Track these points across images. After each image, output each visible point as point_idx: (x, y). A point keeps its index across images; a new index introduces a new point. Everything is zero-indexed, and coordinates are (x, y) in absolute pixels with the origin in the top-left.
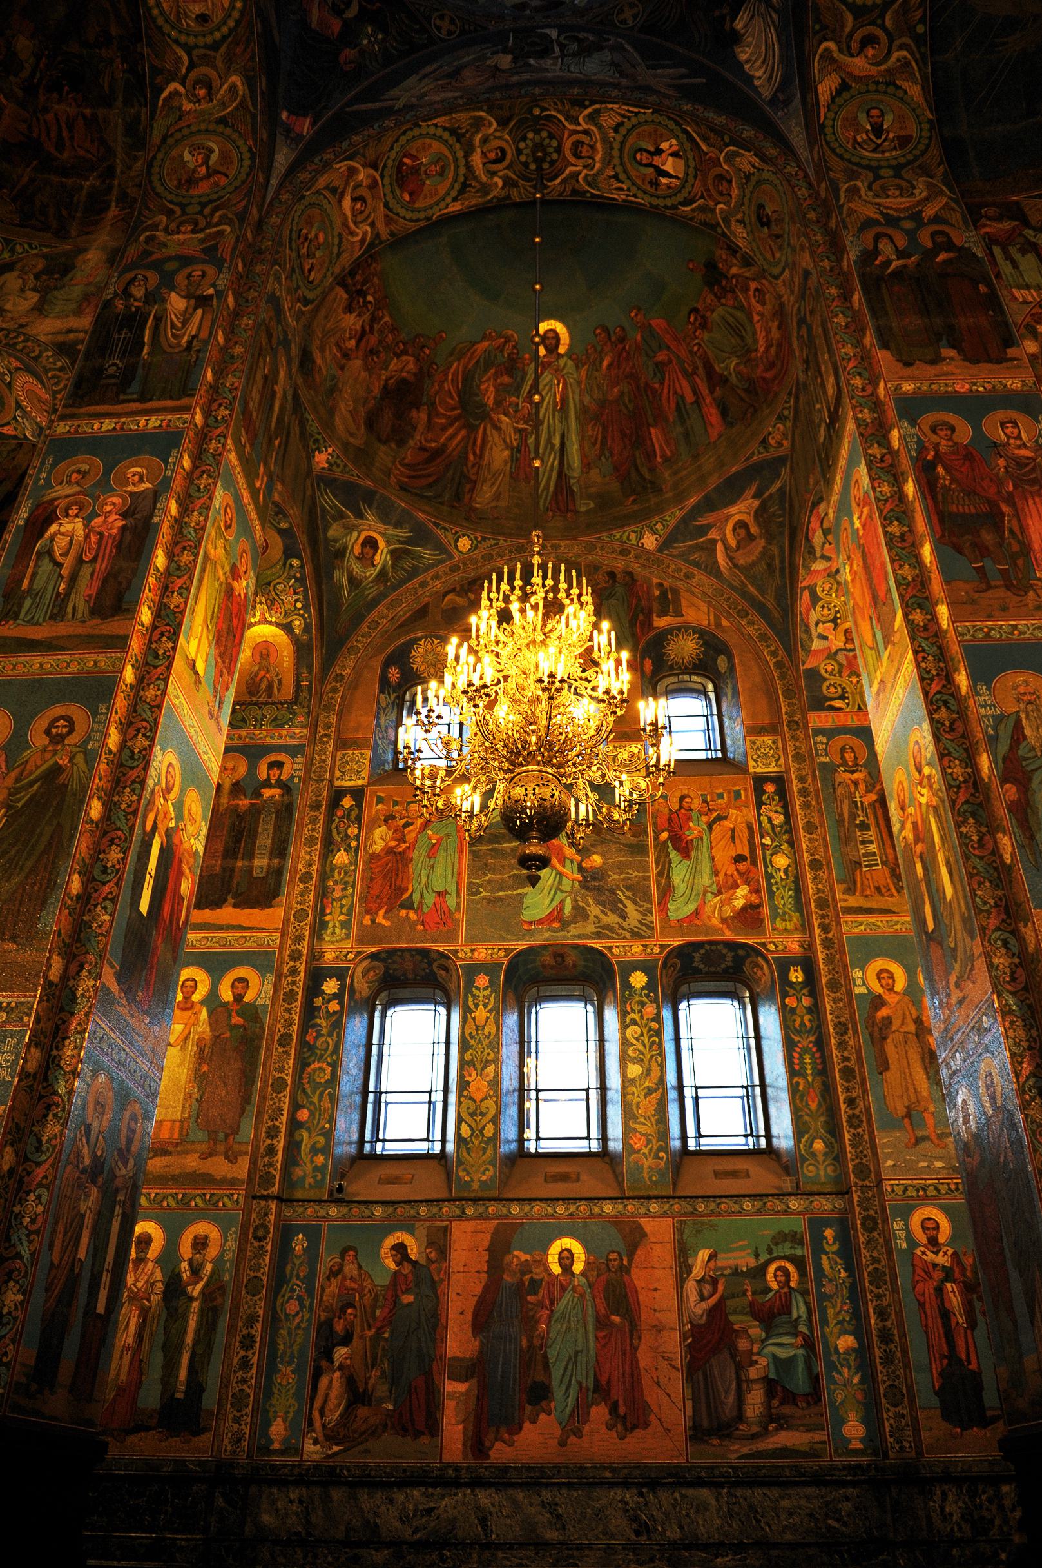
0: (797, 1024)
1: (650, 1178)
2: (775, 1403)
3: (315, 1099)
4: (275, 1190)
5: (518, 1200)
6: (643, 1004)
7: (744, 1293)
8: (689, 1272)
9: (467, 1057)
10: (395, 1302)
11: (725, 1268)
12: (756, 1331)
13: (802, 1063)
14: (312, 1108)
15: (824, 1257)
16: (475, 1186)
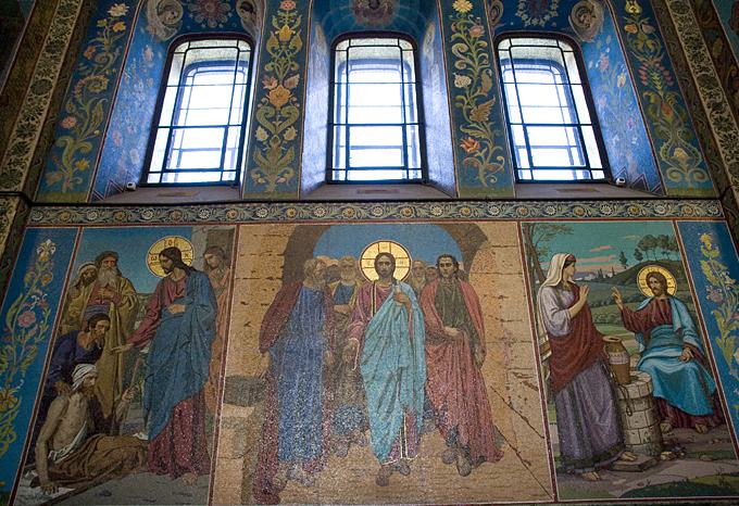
0: (640, 47)
1: (488, 181)
2: (666, 426)
3: (87, 108)
4: (20, 187)
5: (324, 202)
6: (470, 26)
7: (613, 302)
8: (543, 278)
9: (268, 68)
10: (160, 313)
11: (587, 274)
12: (632, 343)
13: (650, 78)
14: (82, 116)
15: (702, 262)
16: (271, 187)
